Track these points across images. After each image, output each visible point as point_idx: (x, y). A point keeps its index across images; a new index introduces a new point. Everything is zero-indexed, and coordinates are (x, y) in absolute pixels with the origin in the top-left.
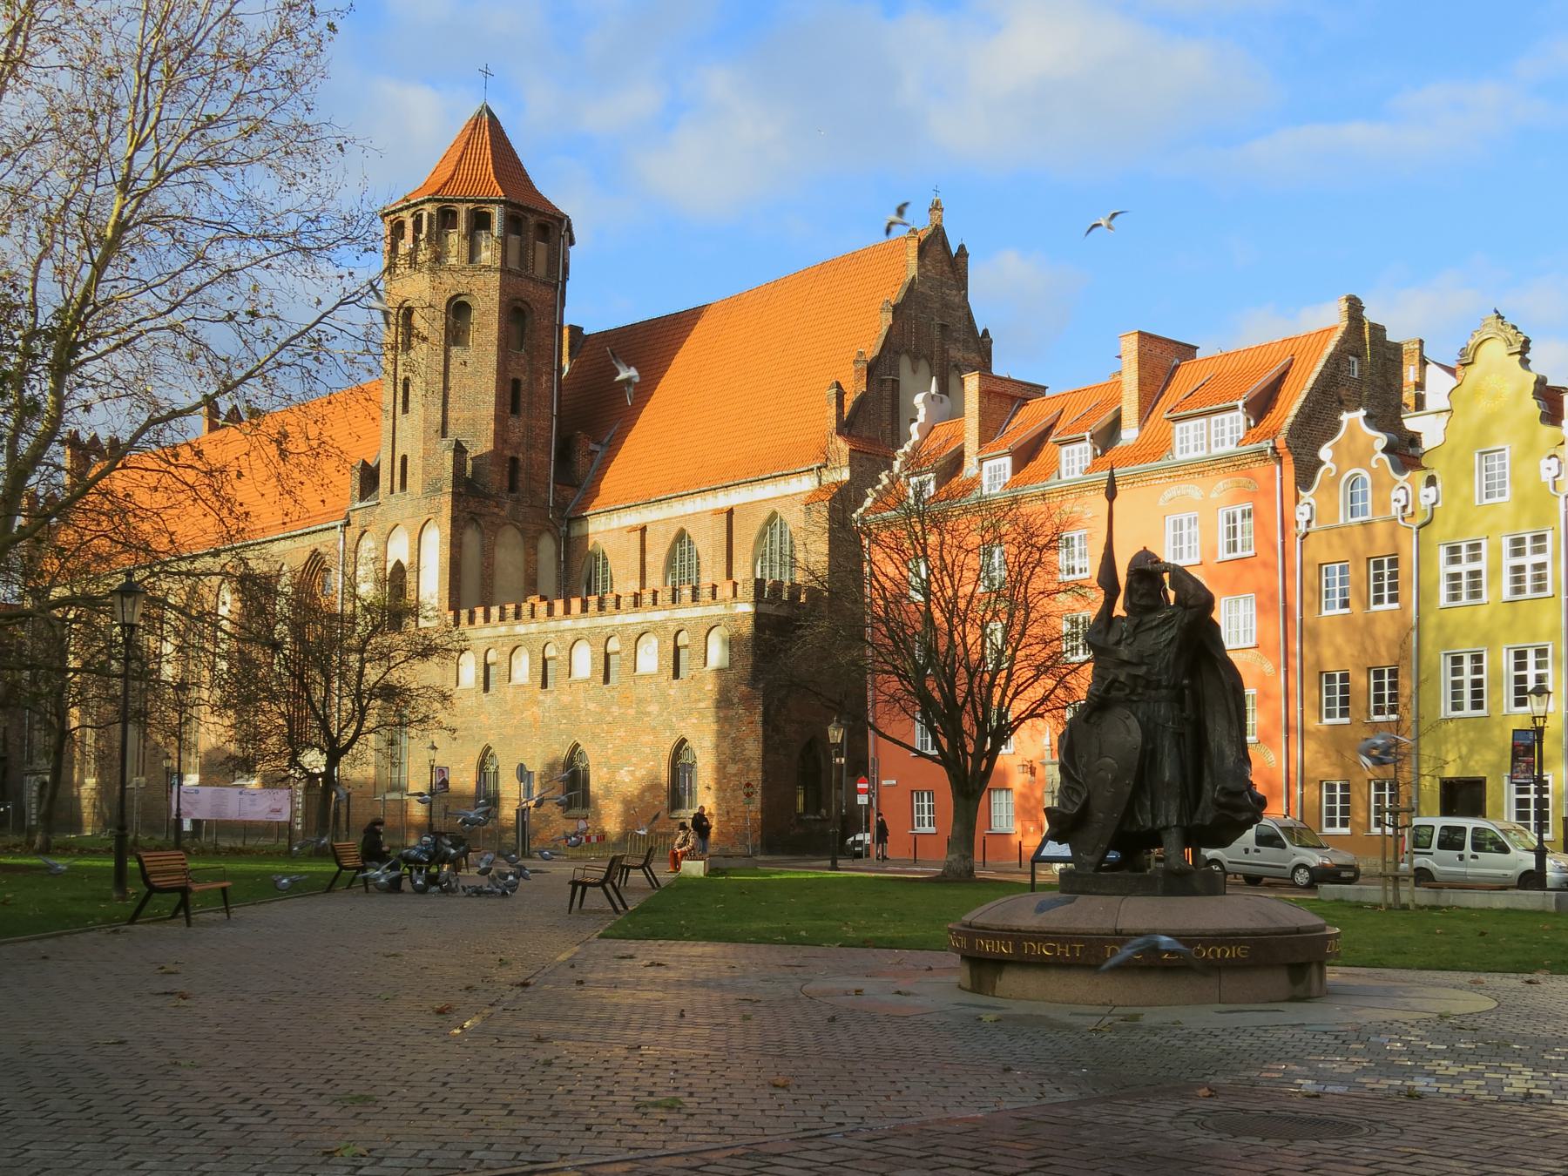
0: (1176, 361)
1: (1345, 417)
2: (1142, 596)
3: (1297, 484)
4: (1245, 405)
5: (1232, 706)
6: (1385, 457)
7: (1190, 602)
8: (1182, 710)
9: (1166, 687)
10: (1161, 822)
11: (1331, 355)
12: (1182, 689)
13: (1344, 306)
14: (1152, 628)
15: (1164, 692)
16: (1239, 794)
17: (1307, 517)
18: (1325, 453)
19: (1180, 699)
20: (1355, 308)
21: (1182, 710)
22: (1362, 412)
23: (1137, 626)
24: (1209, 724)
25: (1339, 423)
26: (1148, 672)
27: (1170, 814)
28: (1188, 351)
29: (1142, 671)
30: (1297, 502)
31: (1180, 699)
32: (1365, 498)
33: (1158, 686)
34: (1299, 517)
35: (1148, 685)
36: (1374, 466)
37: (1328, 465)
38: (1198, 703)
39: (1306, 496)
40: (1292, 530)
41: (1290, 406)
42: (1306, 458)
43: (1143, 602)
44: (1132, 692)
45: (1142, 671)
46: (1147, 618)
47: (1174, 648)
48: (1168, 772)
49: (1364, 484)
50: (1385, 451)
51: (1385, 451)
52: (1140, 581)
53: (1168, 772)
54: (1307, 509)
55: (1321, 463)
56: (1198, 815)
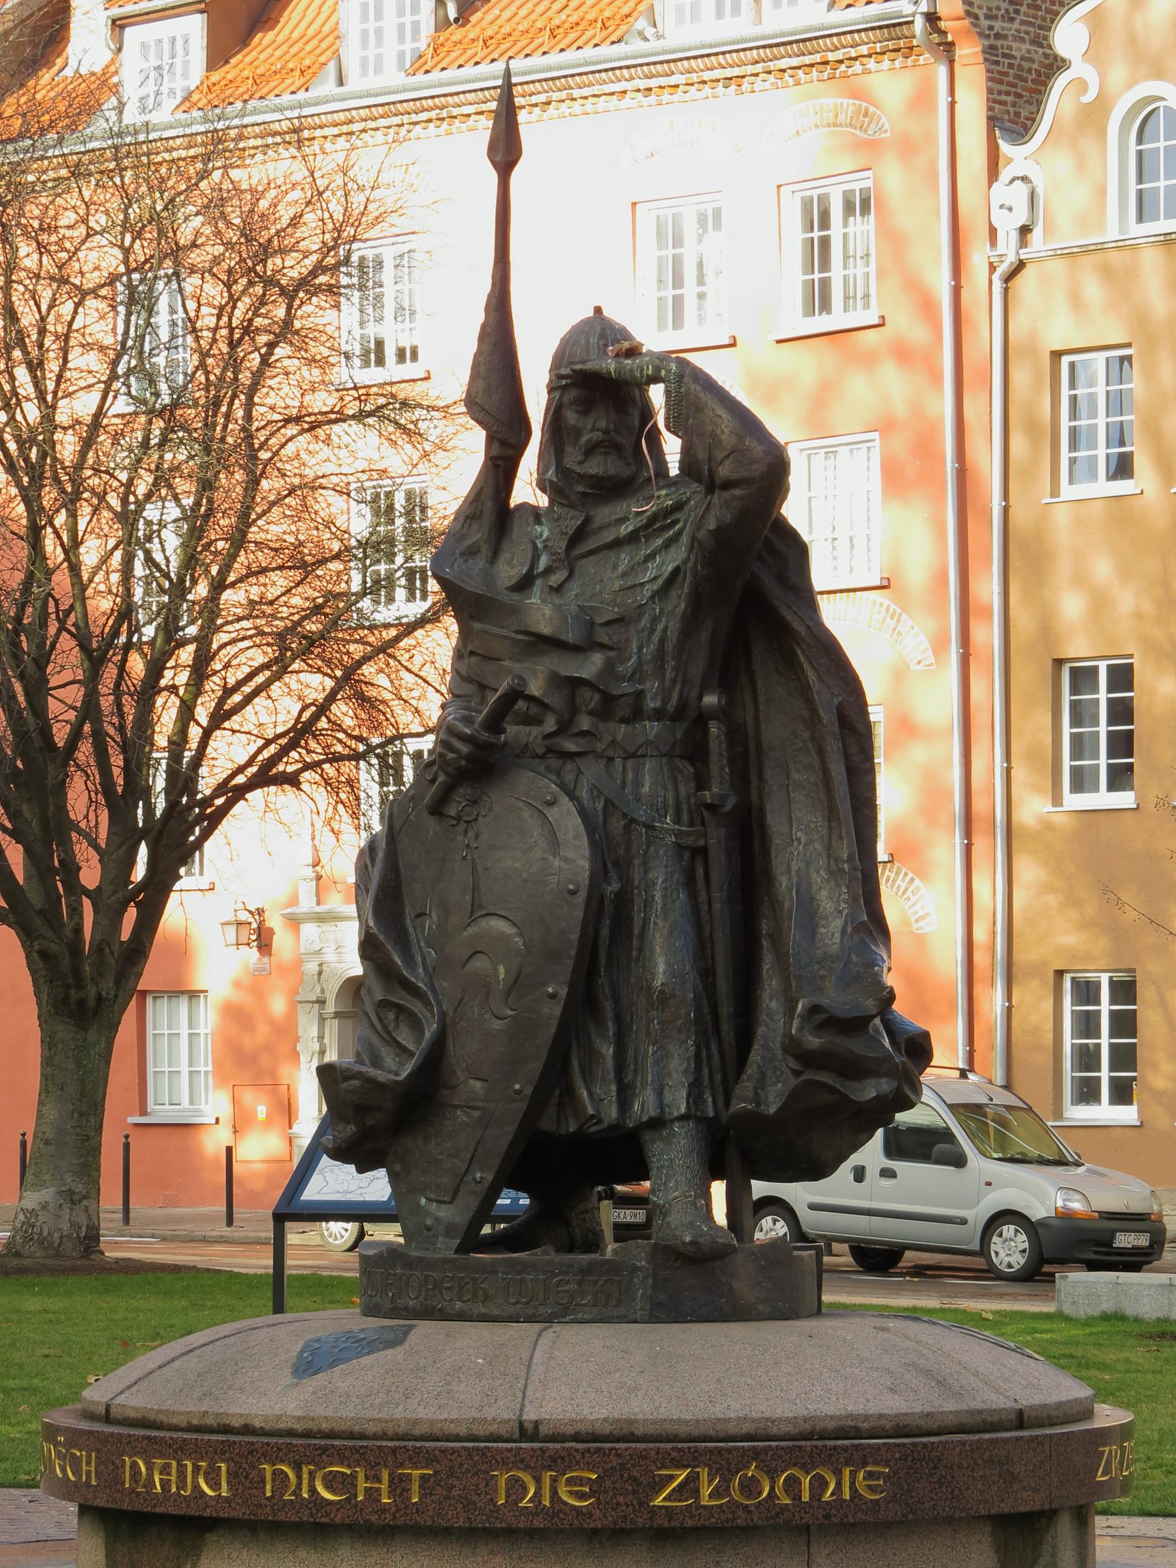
2: (590, 450)
3: (993, 121)
5: (838, 770)
7: (725, 471)
8: (701, 783)
9: (659, 714)
10: (644, 1106)
12: (702, 720)
14: (617, 544)
15: (652, 728)
16: (857, 1025)
17: (1022, 218)
19: (695, 751)
21: (701, 783)
23: (576, 538)
24: (775, 821)
26: (609, 668)
27: (667, 1083)
29: (590, 666)
30: (993, 172)
31: (695, 751)
33: (637, 713)
35: (607, 707)
37: (1079, 69)
38: (746, 761)
40: (978, 258)
42: (1020, 49)
43: (594, 467)
44: (564, 728)
45: (590, 666)
46: (604, 513)
47: (678, 603)
48: (664, 960)
52: (586, 407)
53: (664, 960)
56: (746, 1086)
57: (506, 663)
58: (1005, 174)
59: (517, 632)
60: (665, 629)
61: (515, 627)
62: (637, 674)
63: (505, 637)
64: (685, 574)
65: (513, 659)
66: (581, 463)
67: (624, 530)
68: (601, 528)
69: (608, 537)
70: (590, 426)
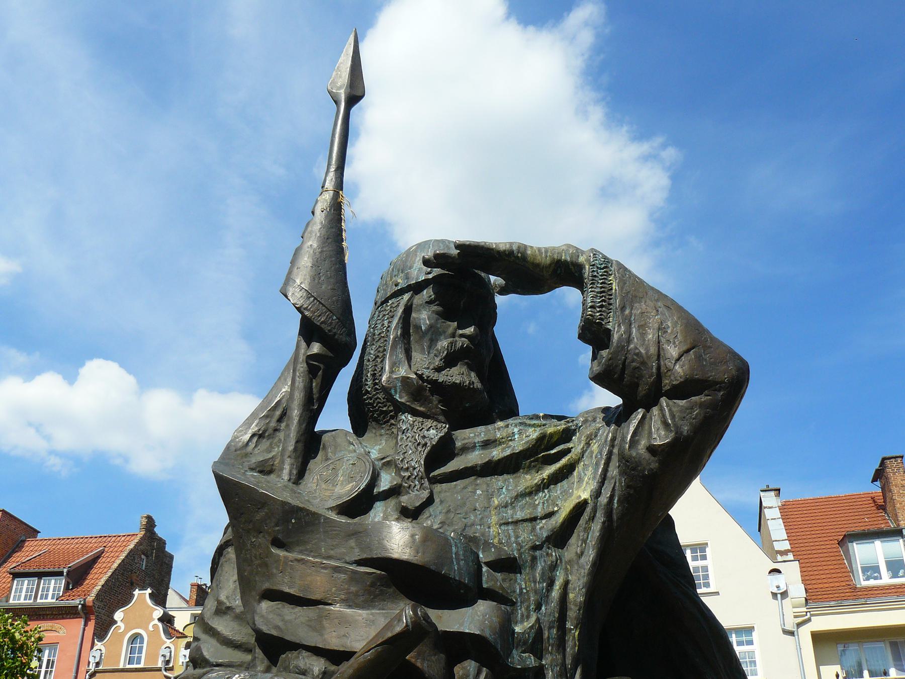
0: (23, 538)
1: (137, 592)
3: (94, 634)
4: (68, 572)
6: (160, 625)
11: (131, 551)
13: (144, 521)
17: (97, 660)
18: (118, 615)
20: (150, 523)
22: (149, 591)
25: (133, 595)
26: (506, 627)
28: (35, 532)
29: (472, 619)
30: (92, 648)
32: (140, 652)
34: (92, 660)
36: (151, 628)
37: (119, 623)
39: (99, 645)
40: (83, 669)
41: (98, 580)
42: (104, 617)
49: (142, 642)
50: (159, 620)
51: (159, 620)
54: (97, 654)
55: (116, 622)
57: (337, 608)
58: (95, 648)
59: (360, 563)
60: (566, 583)
61: (357, 555)
62: (536, 645)
63: (336, 569)
64: (595, 510)
65: (349, 602)
66: (438, 370)
67: (497, 453)
68: (466, 449)
69: (476, 458)
70: (451, 330)
